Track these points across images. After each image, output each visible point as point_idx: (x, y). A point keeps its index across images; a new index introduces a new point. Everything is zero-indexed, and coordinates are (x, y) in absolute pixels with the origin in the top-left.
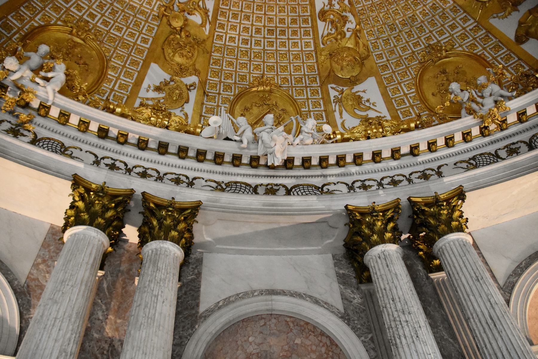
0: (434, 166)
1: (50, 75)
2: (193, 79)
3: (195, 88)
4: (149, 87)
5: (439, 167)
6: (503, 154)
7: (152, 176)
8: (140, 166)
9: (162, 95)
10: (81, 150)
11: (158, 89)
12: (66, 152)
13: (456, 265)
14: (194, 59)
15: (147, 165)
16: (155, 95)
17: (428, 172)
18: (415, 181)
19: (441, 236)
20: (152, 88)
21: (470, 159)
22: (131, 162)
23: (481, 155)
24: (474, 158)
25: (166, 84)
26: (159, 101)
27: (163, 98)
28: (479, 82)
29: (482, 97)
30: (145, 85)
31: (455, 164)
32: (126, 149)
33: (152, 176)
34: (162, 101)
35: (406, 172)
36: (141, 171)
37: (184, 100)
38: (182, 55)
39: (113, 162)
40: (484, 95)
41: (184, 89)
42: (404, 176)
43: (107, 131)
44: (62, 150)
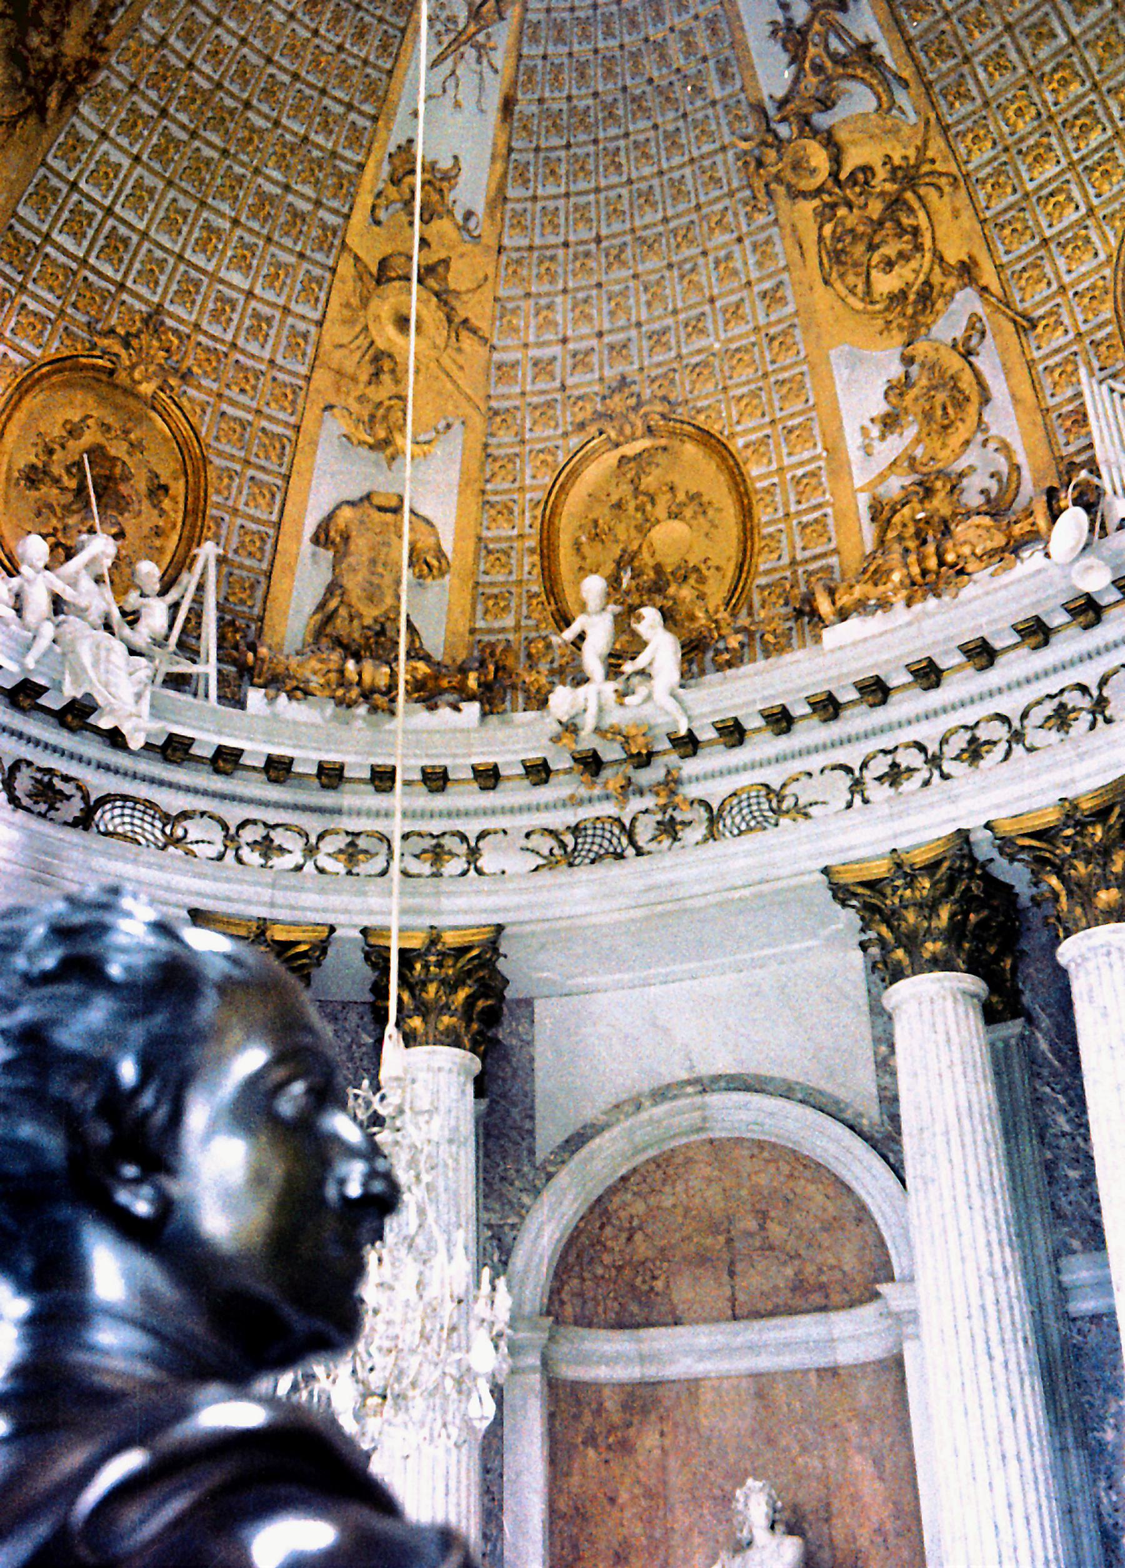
1: (641, 661)
2: (967, 302)
3: (983, 334)
4: (864, 430)
7: (995, 743)
8: (953, 732)
9: (911, 432)
10: (810, 774)
11: (890, 423)
12: (784, 806)
14: (928, 243)
15: (969, 716)
16: (894, 446)
20: (875, 432)
22: (929, 733)
25: (897, 389)
26: (912, 460)
27: (918, 441)
30: (853, 441)
32: (900, 707)
33: (995, 743)
34: (919, 452)
36: (964, 745)
37: (975, 399)
38: (889, 265)
39: (889, 759)
41: (955, 363)
43: (831, 698)
44: (774, 805)
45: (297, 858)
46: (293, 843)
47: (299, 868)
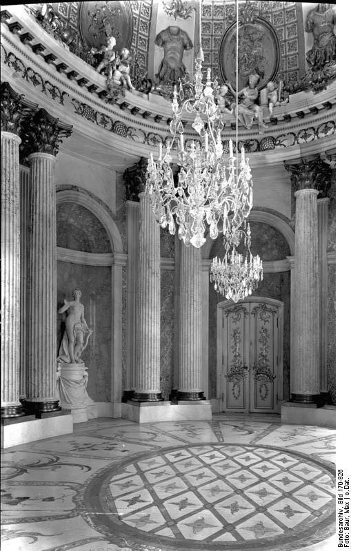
0: (63, 88)
5: (64, 93)
6: (99, 117)
13: (45, 178)
17: (57, 91)
18: (47, 91)
19: (44, 151)
21: (82, 104)
23: (89, 107)
24: (84, 105)
28: (123, 52)
29: (117, 67)
31: (73, 100)
35: (46, 77)
40: (120, 67)
42: (42, 80)
45: (312, 137)
46: (312, 132)
47: (313, 139)
